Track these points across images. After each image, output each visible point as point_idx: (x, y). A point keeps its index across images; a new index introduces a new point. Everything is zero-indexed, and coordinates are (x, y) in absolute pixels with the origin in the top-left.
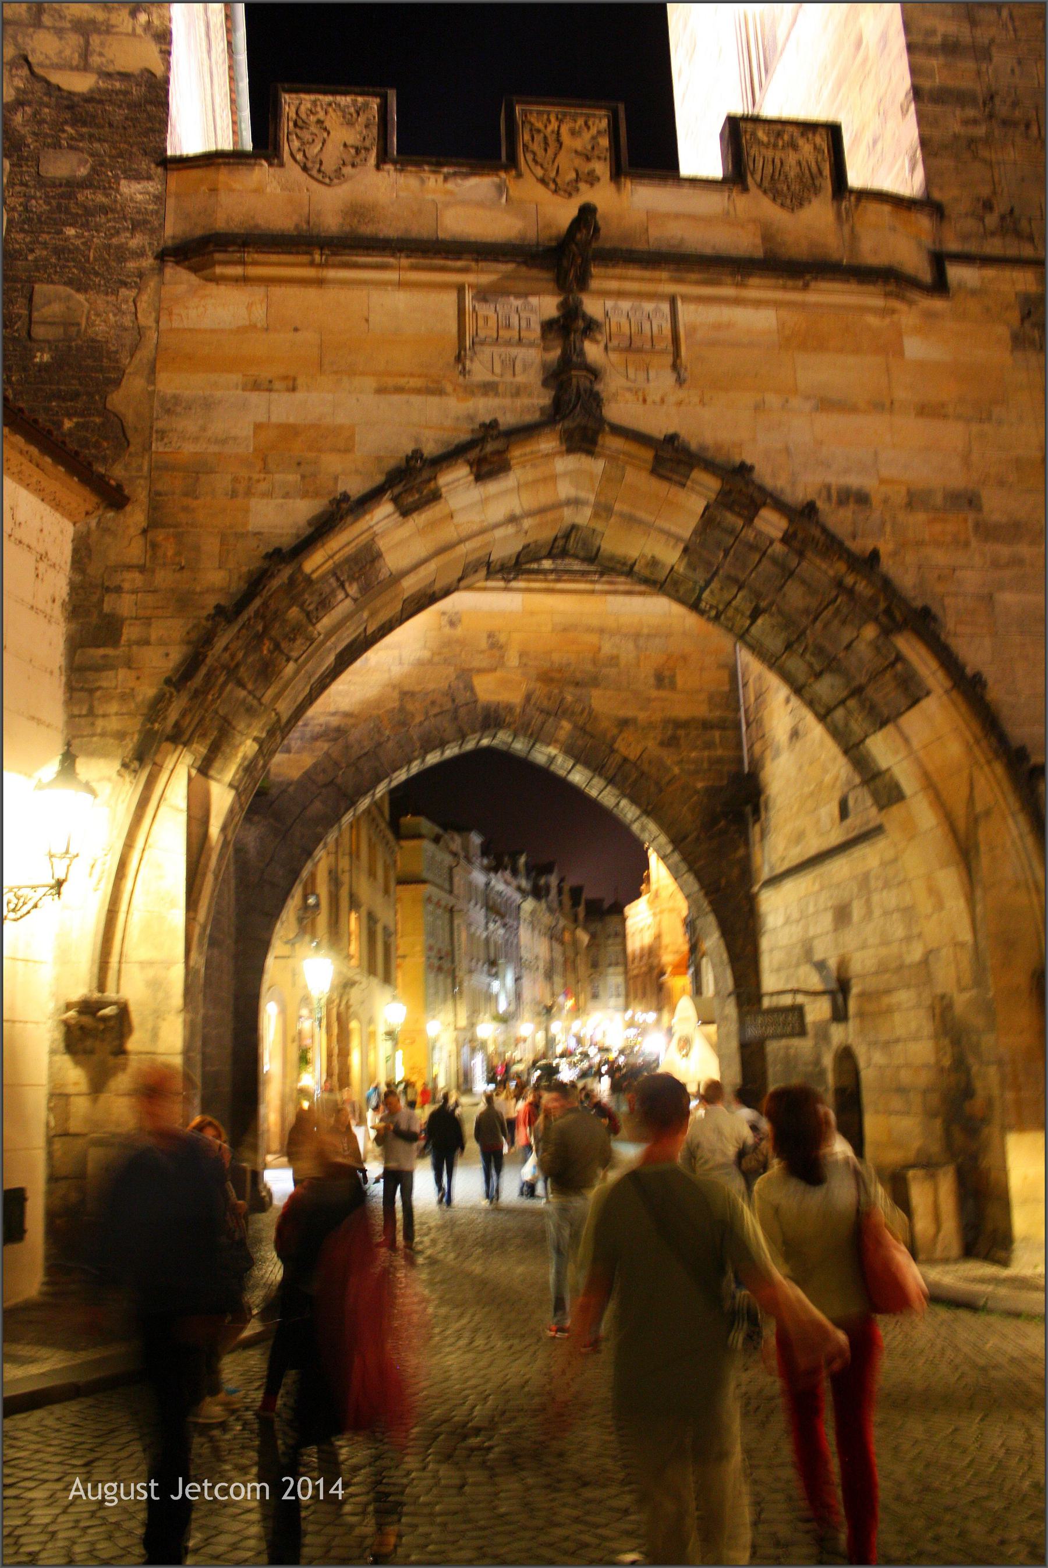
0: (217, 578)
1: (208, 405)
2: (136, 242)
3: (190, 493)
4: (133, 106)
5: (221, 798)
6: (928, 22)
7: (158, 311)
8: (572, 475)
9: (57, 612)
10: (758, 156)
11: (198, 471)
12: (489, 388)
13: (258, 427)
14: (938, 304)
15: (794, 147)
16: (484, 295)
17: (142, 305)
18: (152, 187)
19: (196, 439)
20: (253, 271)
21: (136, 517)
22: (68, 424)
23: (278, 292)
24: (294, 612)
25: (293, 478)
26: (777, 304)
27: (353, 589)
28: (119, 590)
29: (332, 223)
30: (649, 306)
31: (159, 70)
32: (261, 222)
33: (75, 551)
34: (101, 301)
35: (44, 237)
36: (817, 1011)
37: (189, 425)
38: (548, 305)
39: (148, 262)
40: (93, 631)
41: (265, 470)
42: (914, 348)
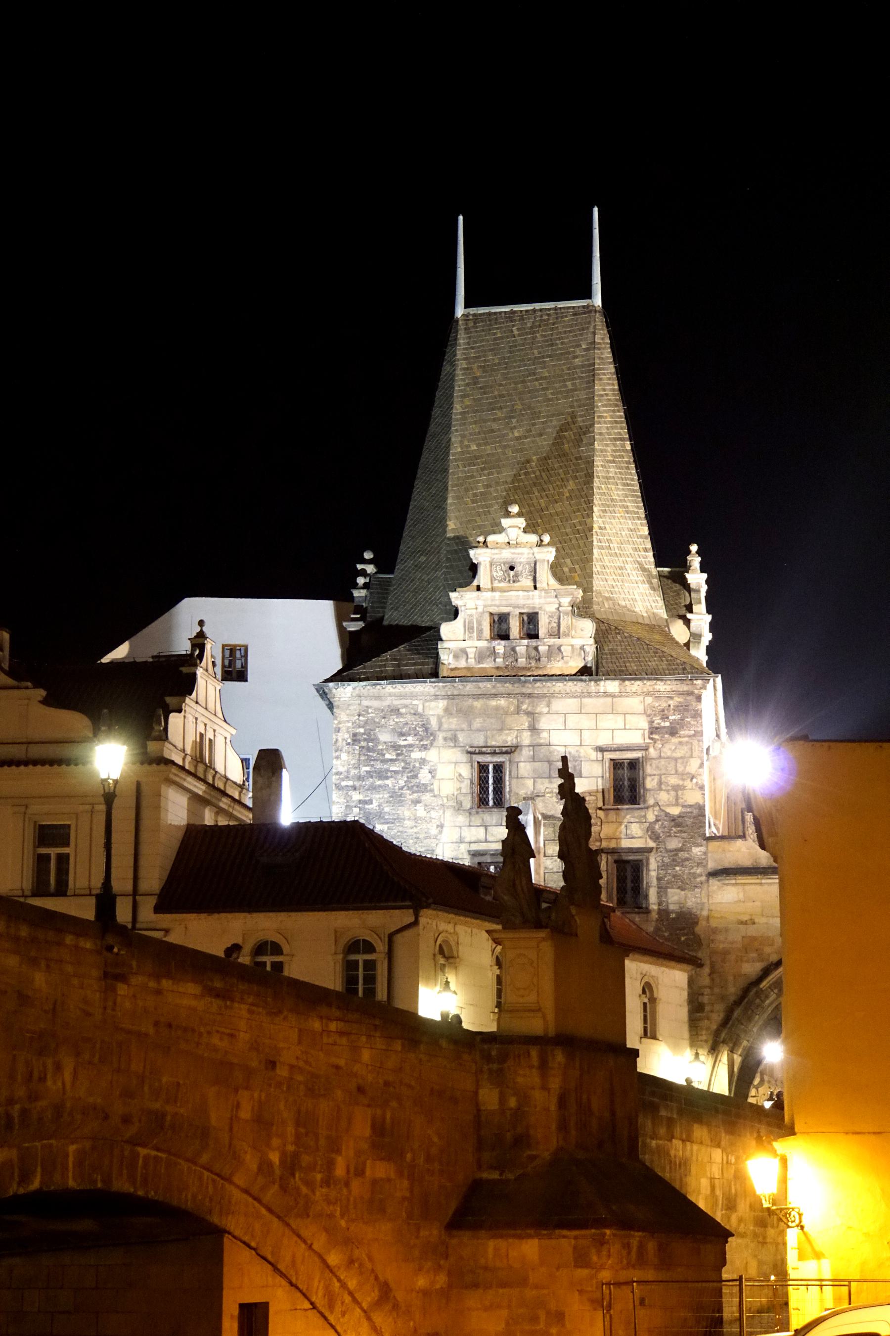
0: (733, 990)
1: (727, 930)
3: (724, 961)
4: (694, 817)
5: (738, 1059)
7: (708, 896)
9: (686, 1004)
11: (726, 953)
13: (743, 937)
17: (703, 895)
18: (703, 849)
19: (723, 943)
20: (738, 882)
21: (706, 970)
22: (683, 939)
23: (747, 887)
24: (758, 1001)
25: (754, 955)
27: (776, 991)
28: (703, 994)
31: (701, 803)
32: (740, 863)
33: (689, 982)
34: (689, 894)
35: (669, 871)
37: (721, 937)
39: (704, 878)
40: (696, 1008)
41: (747, 953)
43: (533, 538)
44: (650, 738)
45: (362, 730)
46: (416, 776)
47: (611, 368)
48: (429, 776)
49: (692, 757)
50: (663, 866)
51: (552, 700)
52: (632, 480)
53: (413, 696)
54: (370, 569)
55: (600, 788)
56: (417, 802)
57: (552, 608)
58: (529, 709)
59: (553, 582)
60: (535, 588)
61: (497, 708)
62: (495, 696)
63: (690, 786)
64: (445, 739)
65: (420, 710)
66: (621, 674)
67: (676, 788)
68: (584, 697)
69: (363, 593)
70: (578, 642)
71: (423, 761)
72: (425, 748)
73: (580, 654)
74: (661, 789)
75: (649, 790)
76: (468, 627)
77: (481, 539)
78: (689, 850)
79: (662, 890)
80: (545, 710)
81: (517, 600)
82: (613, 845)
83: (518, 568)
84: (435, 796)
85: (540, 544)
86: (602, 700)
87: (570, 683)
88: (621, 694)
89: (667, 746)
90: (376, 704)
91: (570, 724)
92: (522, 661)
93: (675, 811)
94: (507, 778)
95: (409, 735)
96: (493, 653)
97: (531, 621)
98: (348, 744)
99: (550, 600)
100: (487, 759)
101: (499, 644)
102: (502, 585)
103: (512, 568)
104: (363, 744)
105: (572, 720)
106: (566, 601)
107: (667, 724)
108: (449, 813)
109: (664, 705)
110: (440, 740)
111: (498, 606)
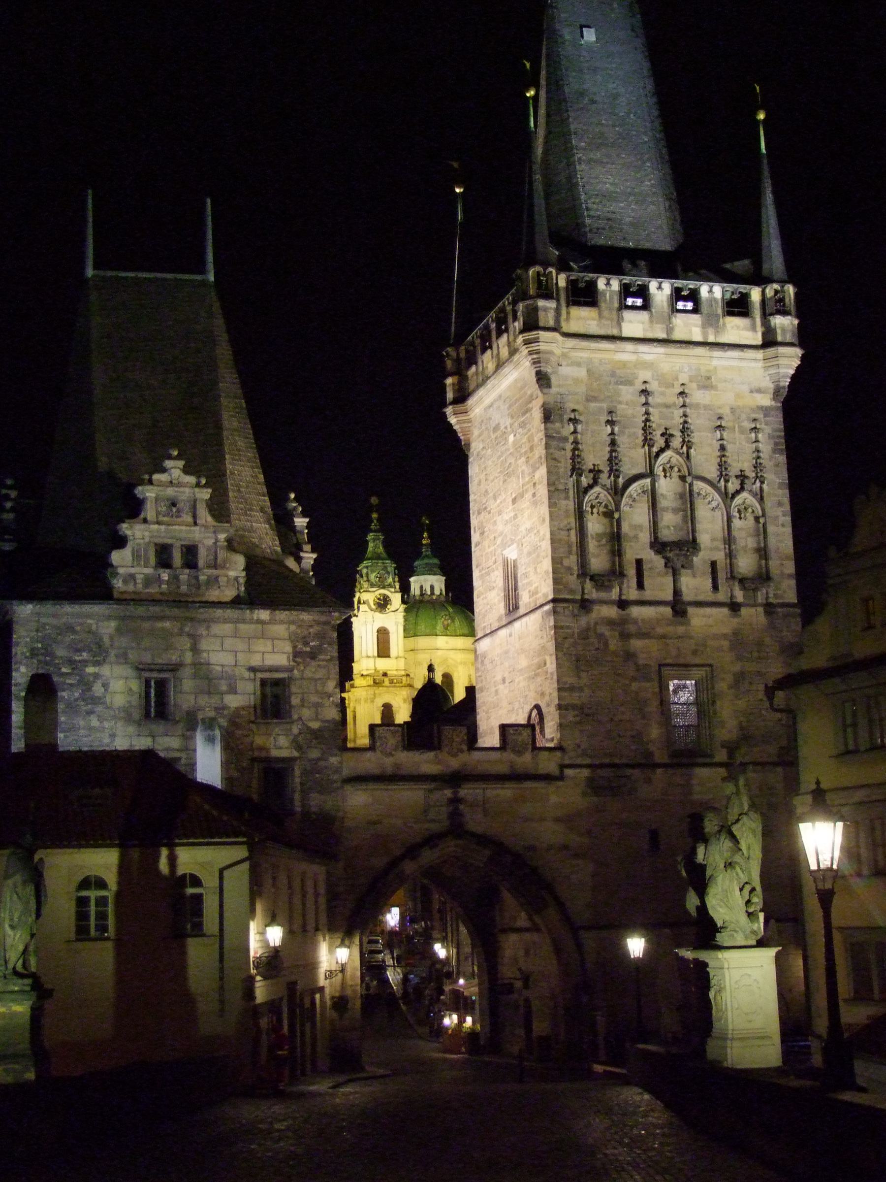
2: (336, 777)
6: (565, 679)
8: (456, 846)
10: (510, 738)
12: (433, 821)
14: (560, 783)
15: (520, 734)
16: (431, 791)
21: (341, 864)
26: (513, 788)
29: (389, 771)
30: (478, 791)
36: (518, 984)
38: (448, 793)
39: (339, 784)
40: (333, 896)
42: (554, 799)
43: (192, 479)
44: (294, 661)
45: (40, 645)
46: (89, 689)
47: (225, 336)
48: (103, 690)
49: (329, 678)
50: (305, 773)
51: (211, 624)
52: (249, 434)
53: (89, 616)
54: (13, 494)
55: (252, 704)
56: (90, 713)
57: (211, 542)
58: (191, 632)
59: (209, 518)
60: (195, 524)
61: (163, 629)
62: (162, 618)
63: (327, 704)
64: (117, 656)
65: (94, 627)
66: (271, 604)
67: (317, 705)
68: (240, 623)
69: (11, 516)
70: (232, 574)
71: (96, 676)
72: (97, 664)
73: (233, 585)
74: (303, 706)
75: (294, 707)
76: (136, 556)
77: (147, 477)
78: (326, 760)
79: (305, 793)
80: (205, 633)
81: (181, 532)
82: (263, 754)
83: (180, 505)
84: (107, 708)
85: (198, 485)
86: (253, 626)
87: (229, 611)
88: (272, 622)
89: (308, 668)
90: (54, 621)
91: (226, 646)
92: (184, 588)
93: (315, 725)
94: (172, 693)
95: (84, 651)
96: (159, 579)
97: (190, 552)
98: (26, 657)
99: (207, 536)
100: (148, 674)
101: (164, 572)
102: (166, 519)
103: (174, 504)
104: (41, 658)
105: (229, 643)
106: (222, 536)
107: (308, 649)
108: (119, 724)
109: (306, 632)
110: (112, 658)
111: (163, 538)
